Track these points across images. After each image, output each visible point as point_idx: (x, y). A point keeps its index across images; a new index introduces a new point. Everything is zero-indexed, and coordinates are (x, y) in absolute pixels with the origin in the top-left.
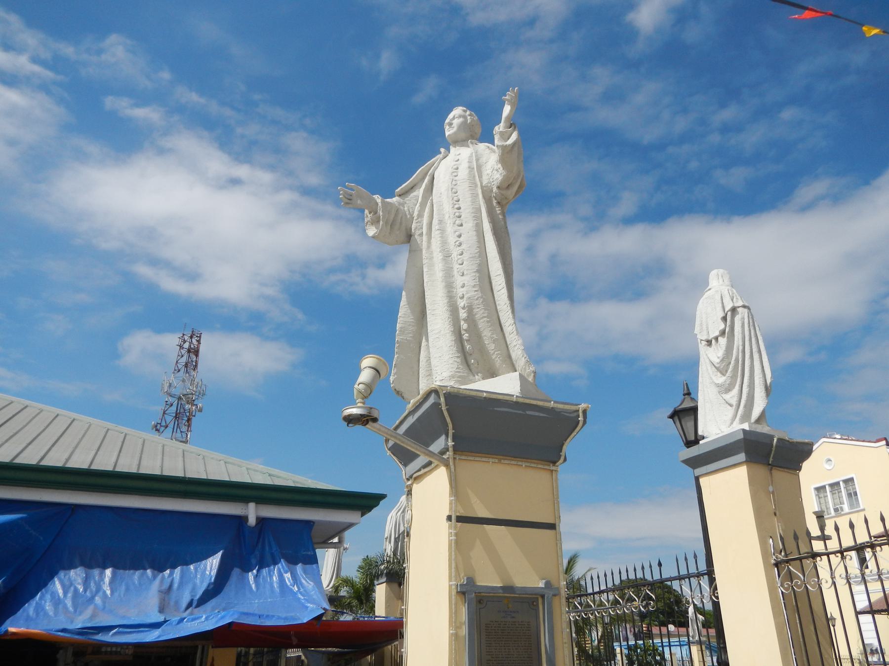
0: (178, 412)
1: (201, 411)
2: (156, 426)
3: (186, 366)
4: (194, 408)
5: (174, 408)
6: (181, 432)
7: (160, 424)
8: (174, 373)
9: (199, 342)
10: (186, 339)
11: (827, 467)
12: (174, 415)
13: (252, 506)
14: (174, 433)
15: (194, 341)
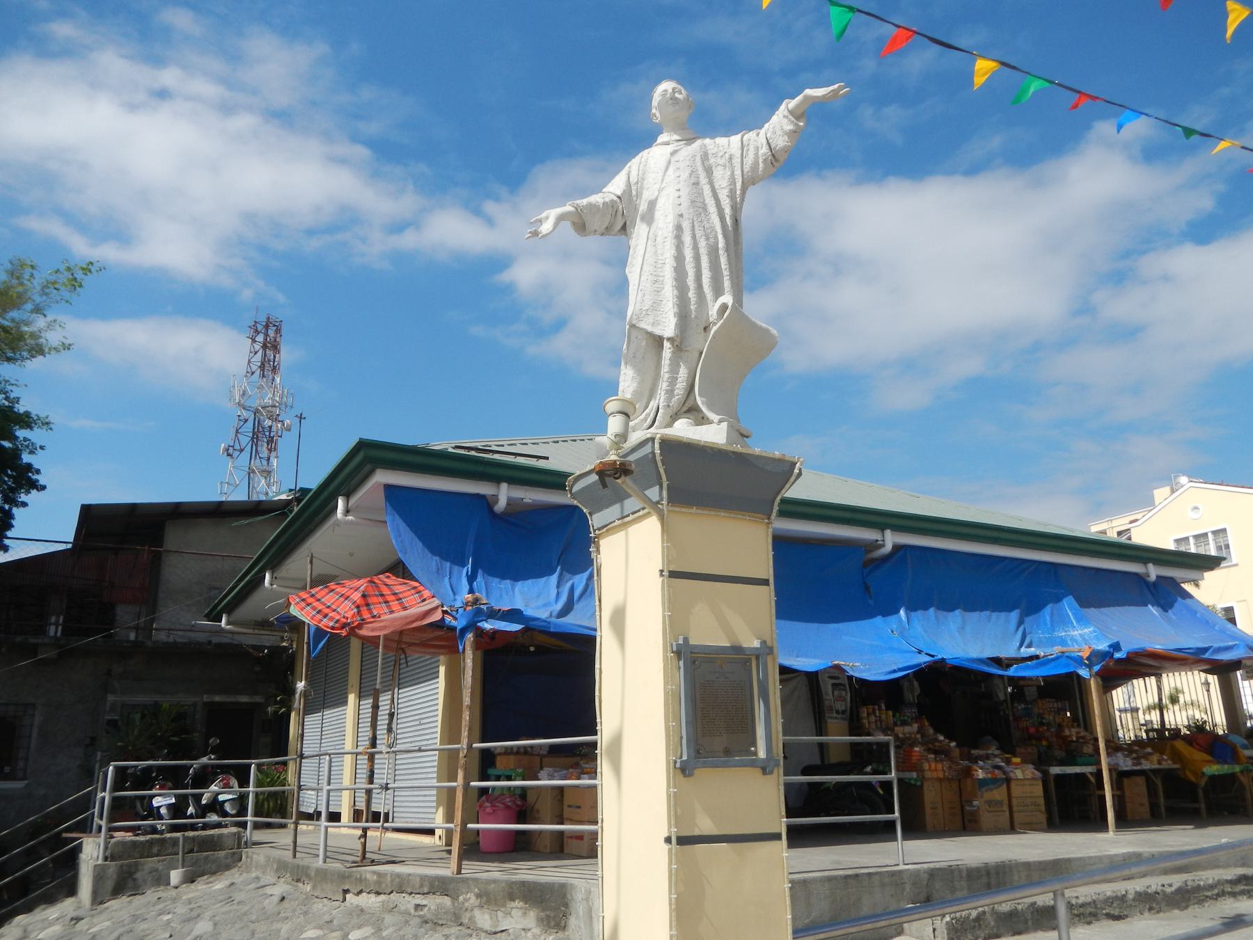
0: (256, 430)
1: (289, 430)
2: (228, 450)
3: (262, 367)
4: (279, 425)
5: (250, 424)
6: (260, 458)
7: (233, 447)
8: (246, 376)
9: (278, 331)
10: (259, 329)
11: (1194, 515)
12: (251, 435)
13: (1151, 566)
14: (253, 459)
15: (271, 332)
